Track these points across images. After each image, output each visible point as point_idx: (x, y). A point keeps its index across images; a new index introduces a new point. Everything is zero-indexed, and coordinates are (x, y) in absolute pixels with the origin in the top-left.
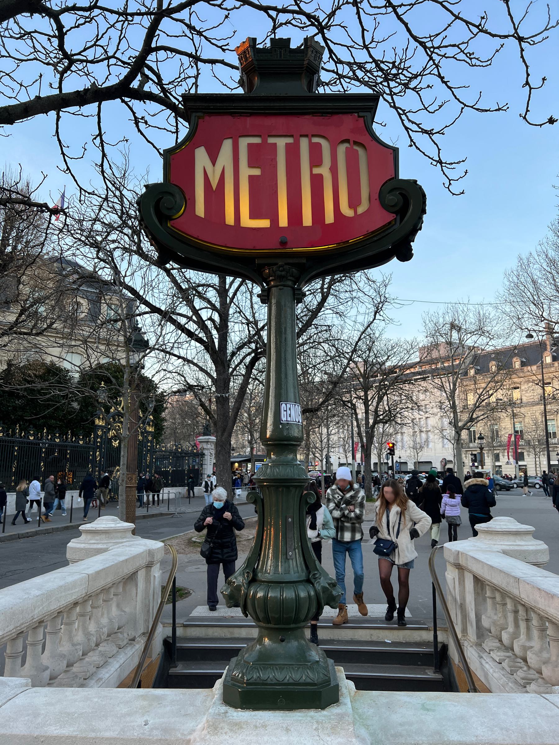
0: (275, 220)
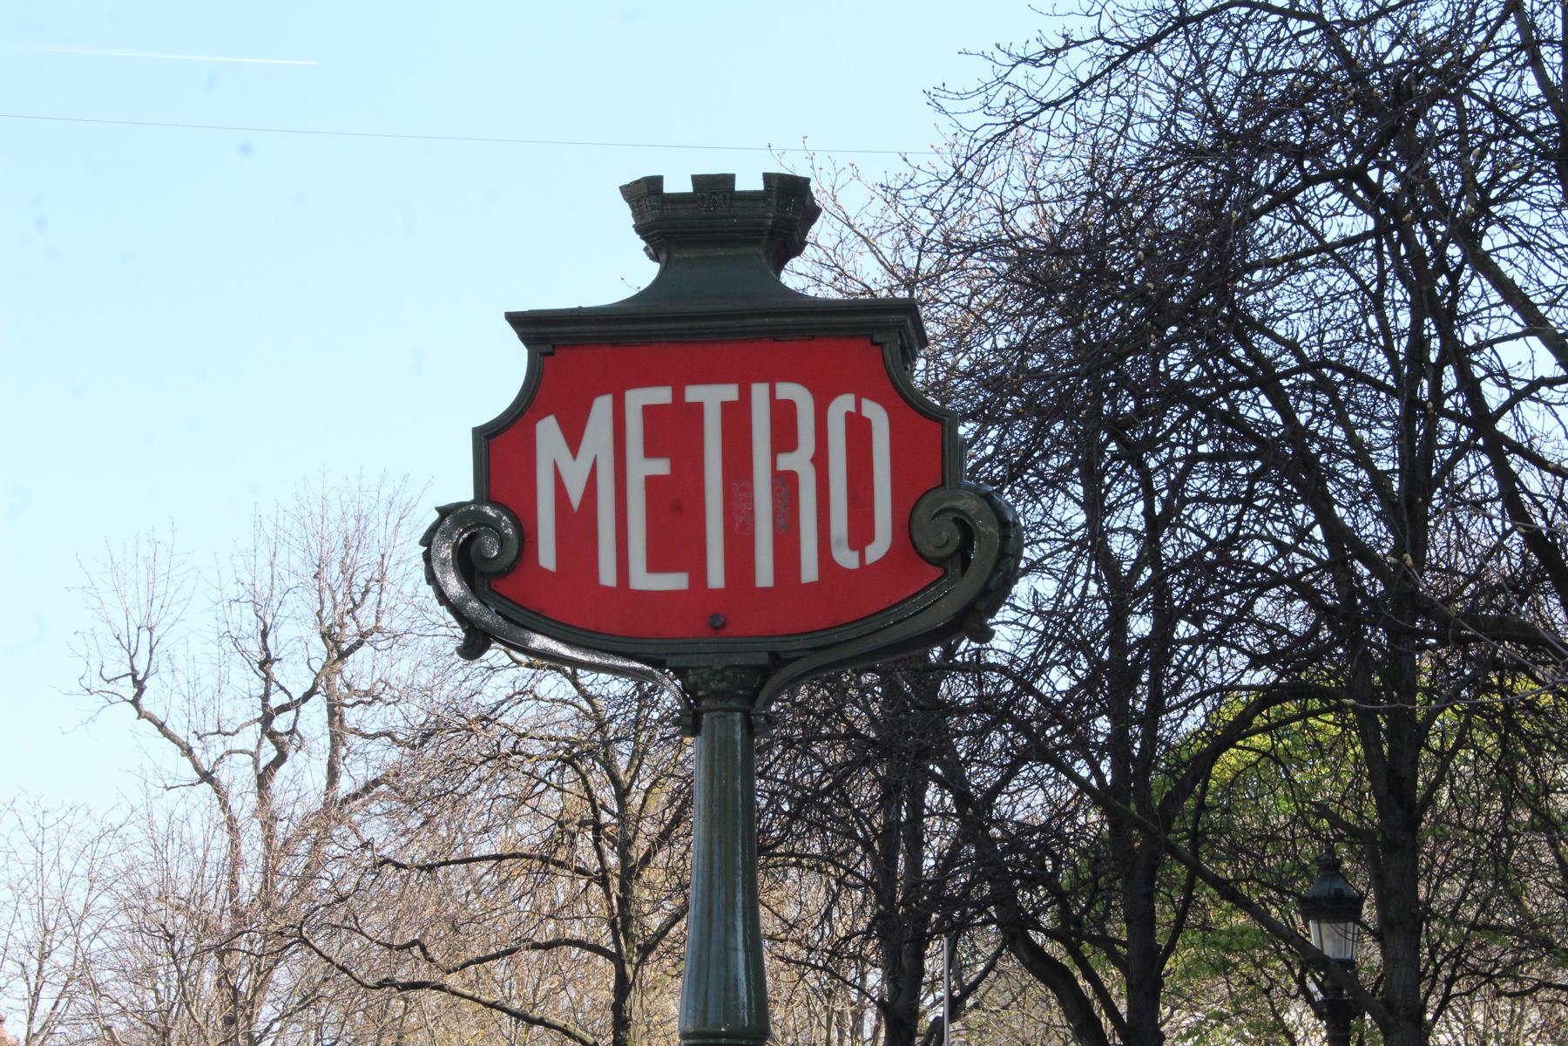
0: (698, 572)
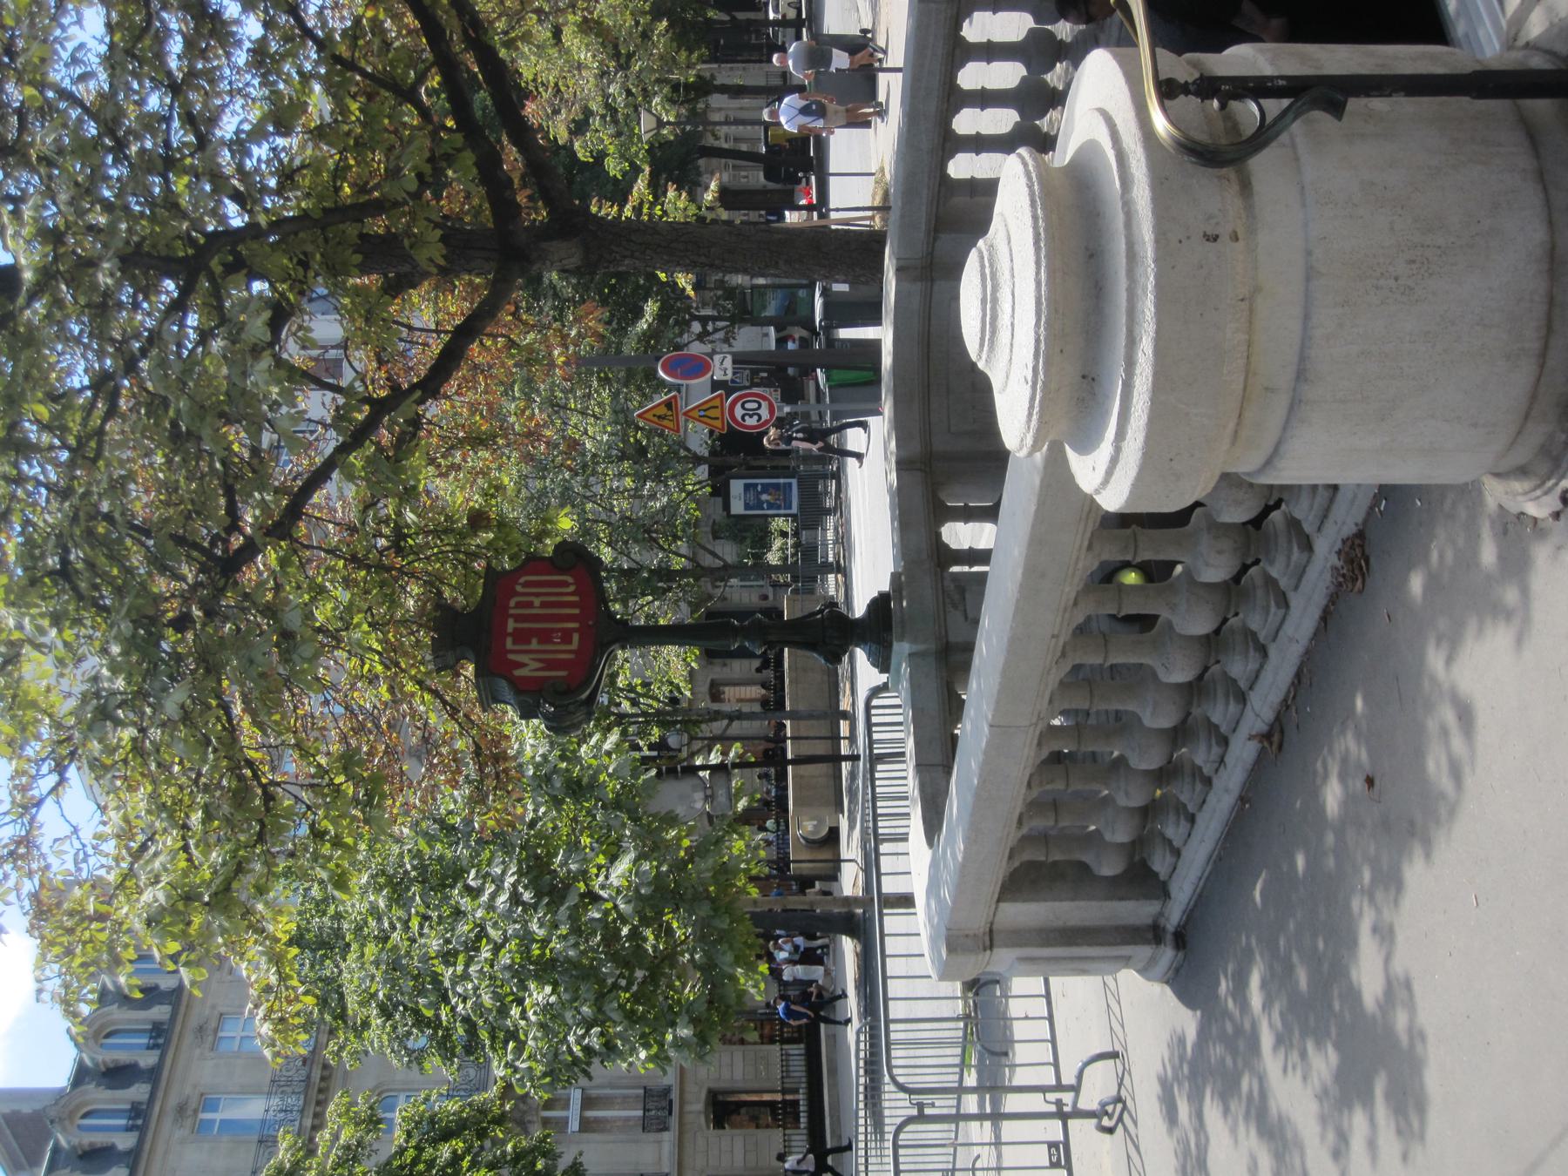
0: (574, 630)
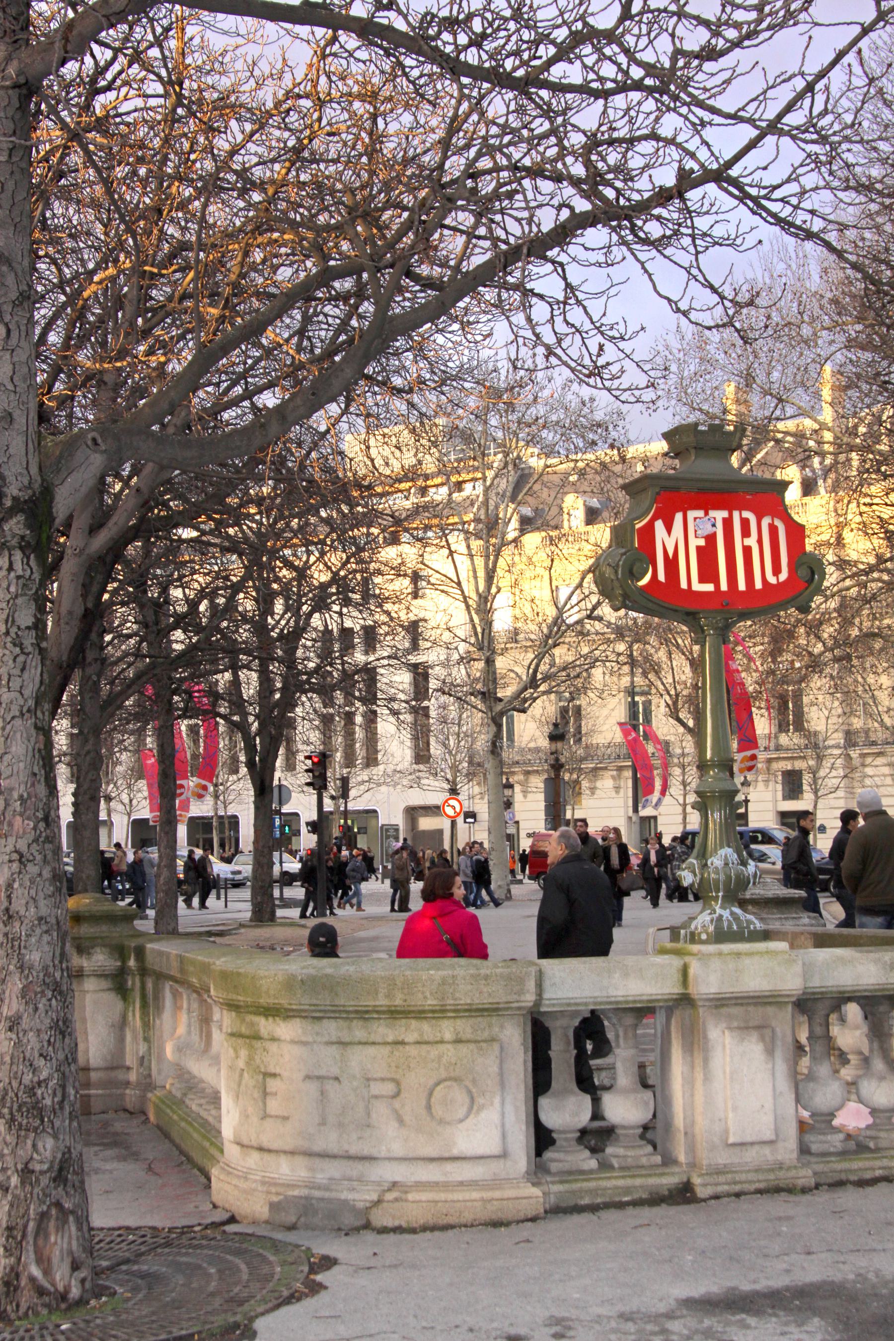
0: (716, 582)
